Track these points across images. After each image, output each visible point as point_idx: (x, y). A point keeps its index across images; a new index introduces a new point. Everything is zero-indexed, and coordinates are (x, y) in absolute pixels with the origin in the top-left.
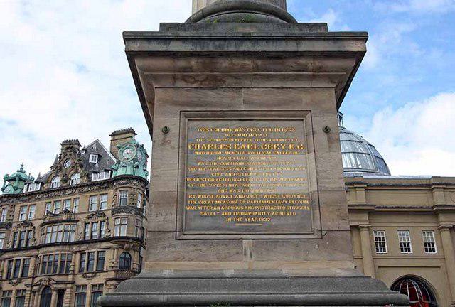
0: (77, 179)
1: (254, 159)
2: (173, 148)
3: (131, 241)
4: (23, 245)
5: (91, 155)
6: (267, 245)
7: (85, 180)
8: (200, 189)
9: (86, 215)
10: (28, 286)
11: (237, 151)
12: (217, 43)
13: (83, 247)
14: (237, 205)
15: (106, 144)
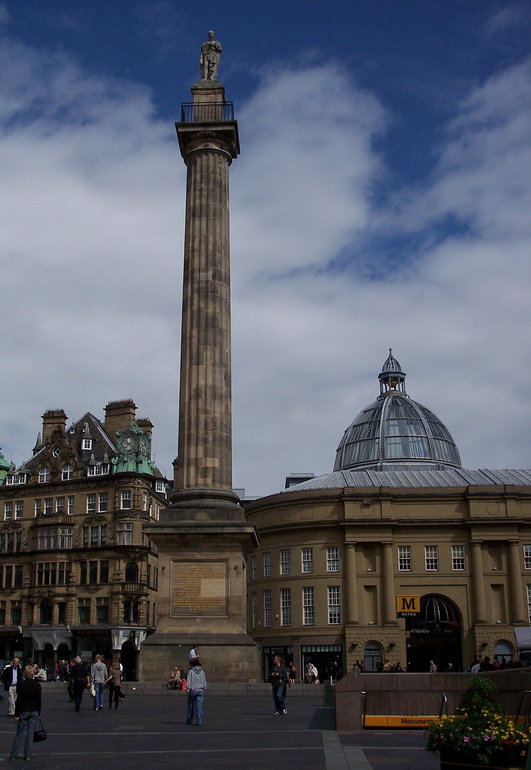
0: (67, 472)
1: (203, 580)
2: (167, 577)
3: (137, 550)
4: (15, 550)
5: (84, 441)
6: (206, 621)
7: (78, 475)
8: (179, 595)
9: (83, 518)
10: (23, 596)
11: (196, 577)
12: (186, 528)
13: (84, 556)
14: (195, 603)
15: (101, 416)
